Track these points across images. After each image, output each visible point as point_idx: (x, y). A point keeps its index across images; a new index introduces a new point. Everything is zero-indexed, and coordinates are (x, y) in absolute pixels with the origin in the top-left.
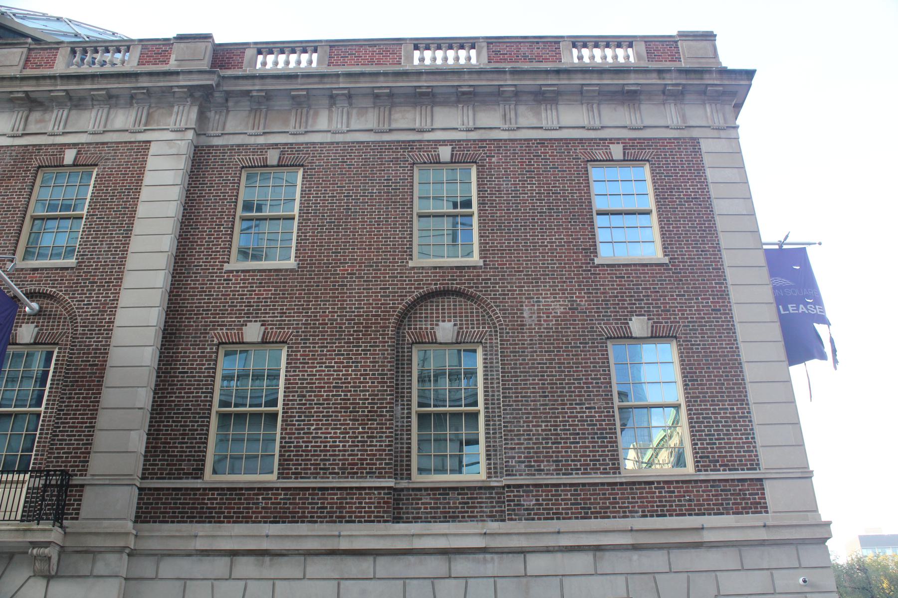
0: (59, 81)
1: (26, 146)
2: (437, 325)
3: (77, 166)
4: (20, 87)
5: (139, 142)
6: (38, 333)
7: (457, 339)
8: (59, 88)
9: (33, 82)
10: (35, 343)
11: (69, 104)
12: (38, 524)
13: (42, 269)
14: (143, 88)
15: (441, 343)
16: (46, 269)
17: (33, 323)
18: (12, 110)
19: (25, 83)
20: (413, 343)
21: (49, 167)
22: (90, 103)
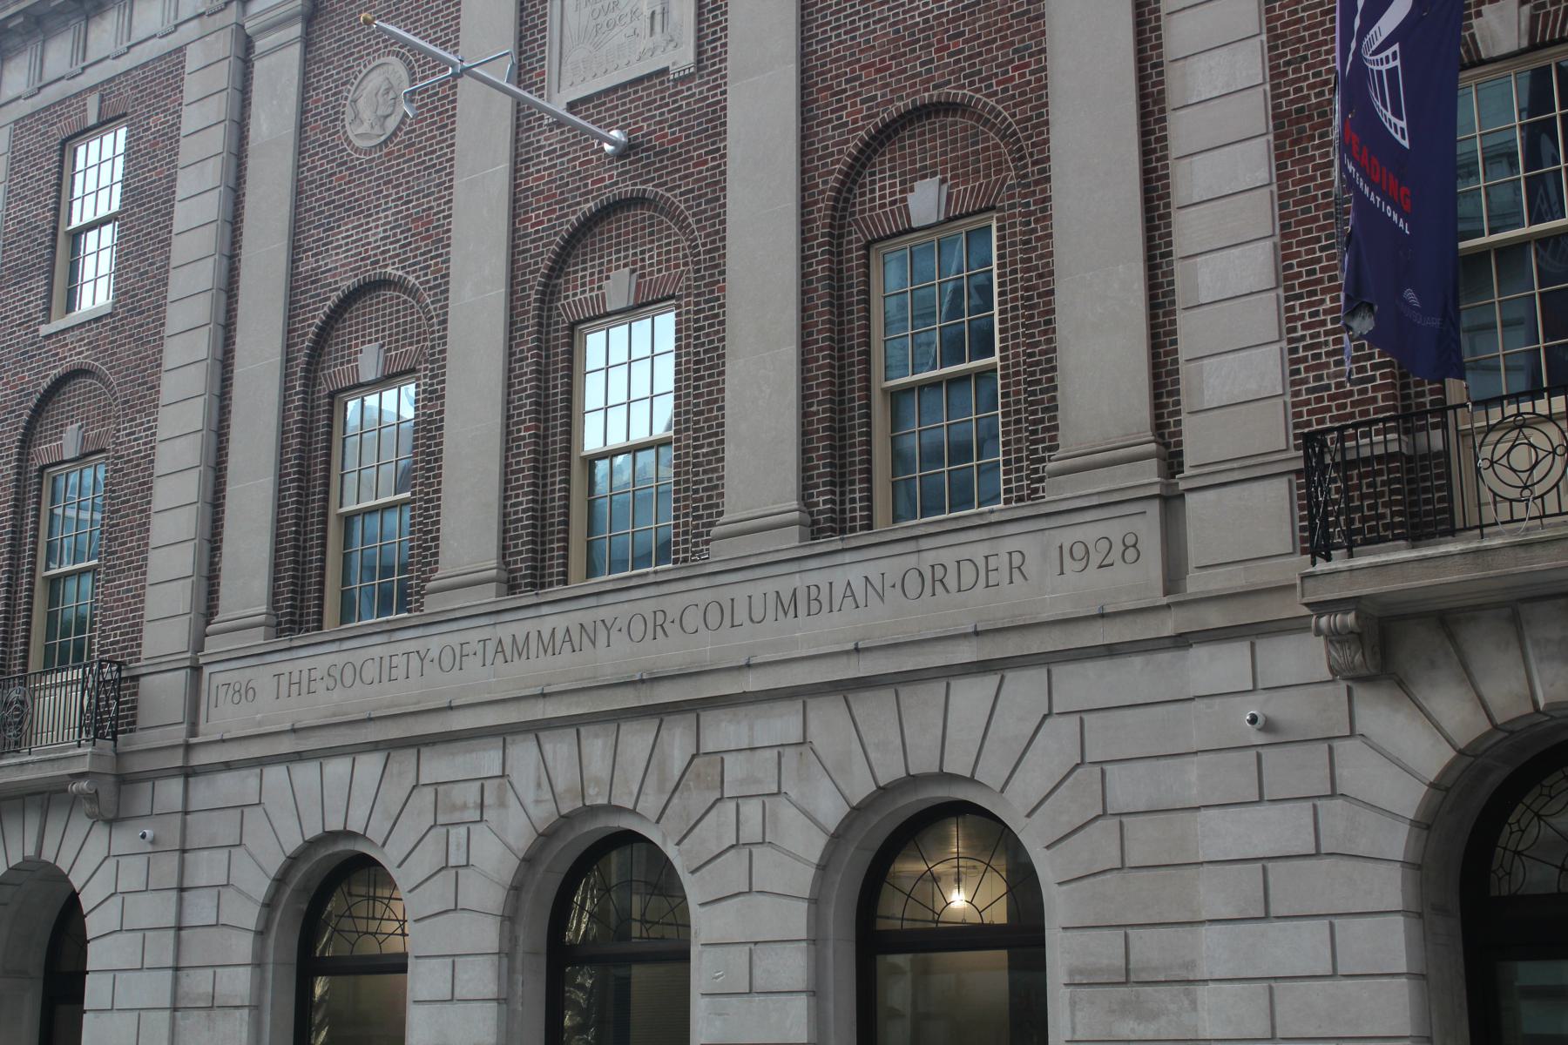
6: (1534, 19)
10: (1533, 47)
12: (1351, 556)
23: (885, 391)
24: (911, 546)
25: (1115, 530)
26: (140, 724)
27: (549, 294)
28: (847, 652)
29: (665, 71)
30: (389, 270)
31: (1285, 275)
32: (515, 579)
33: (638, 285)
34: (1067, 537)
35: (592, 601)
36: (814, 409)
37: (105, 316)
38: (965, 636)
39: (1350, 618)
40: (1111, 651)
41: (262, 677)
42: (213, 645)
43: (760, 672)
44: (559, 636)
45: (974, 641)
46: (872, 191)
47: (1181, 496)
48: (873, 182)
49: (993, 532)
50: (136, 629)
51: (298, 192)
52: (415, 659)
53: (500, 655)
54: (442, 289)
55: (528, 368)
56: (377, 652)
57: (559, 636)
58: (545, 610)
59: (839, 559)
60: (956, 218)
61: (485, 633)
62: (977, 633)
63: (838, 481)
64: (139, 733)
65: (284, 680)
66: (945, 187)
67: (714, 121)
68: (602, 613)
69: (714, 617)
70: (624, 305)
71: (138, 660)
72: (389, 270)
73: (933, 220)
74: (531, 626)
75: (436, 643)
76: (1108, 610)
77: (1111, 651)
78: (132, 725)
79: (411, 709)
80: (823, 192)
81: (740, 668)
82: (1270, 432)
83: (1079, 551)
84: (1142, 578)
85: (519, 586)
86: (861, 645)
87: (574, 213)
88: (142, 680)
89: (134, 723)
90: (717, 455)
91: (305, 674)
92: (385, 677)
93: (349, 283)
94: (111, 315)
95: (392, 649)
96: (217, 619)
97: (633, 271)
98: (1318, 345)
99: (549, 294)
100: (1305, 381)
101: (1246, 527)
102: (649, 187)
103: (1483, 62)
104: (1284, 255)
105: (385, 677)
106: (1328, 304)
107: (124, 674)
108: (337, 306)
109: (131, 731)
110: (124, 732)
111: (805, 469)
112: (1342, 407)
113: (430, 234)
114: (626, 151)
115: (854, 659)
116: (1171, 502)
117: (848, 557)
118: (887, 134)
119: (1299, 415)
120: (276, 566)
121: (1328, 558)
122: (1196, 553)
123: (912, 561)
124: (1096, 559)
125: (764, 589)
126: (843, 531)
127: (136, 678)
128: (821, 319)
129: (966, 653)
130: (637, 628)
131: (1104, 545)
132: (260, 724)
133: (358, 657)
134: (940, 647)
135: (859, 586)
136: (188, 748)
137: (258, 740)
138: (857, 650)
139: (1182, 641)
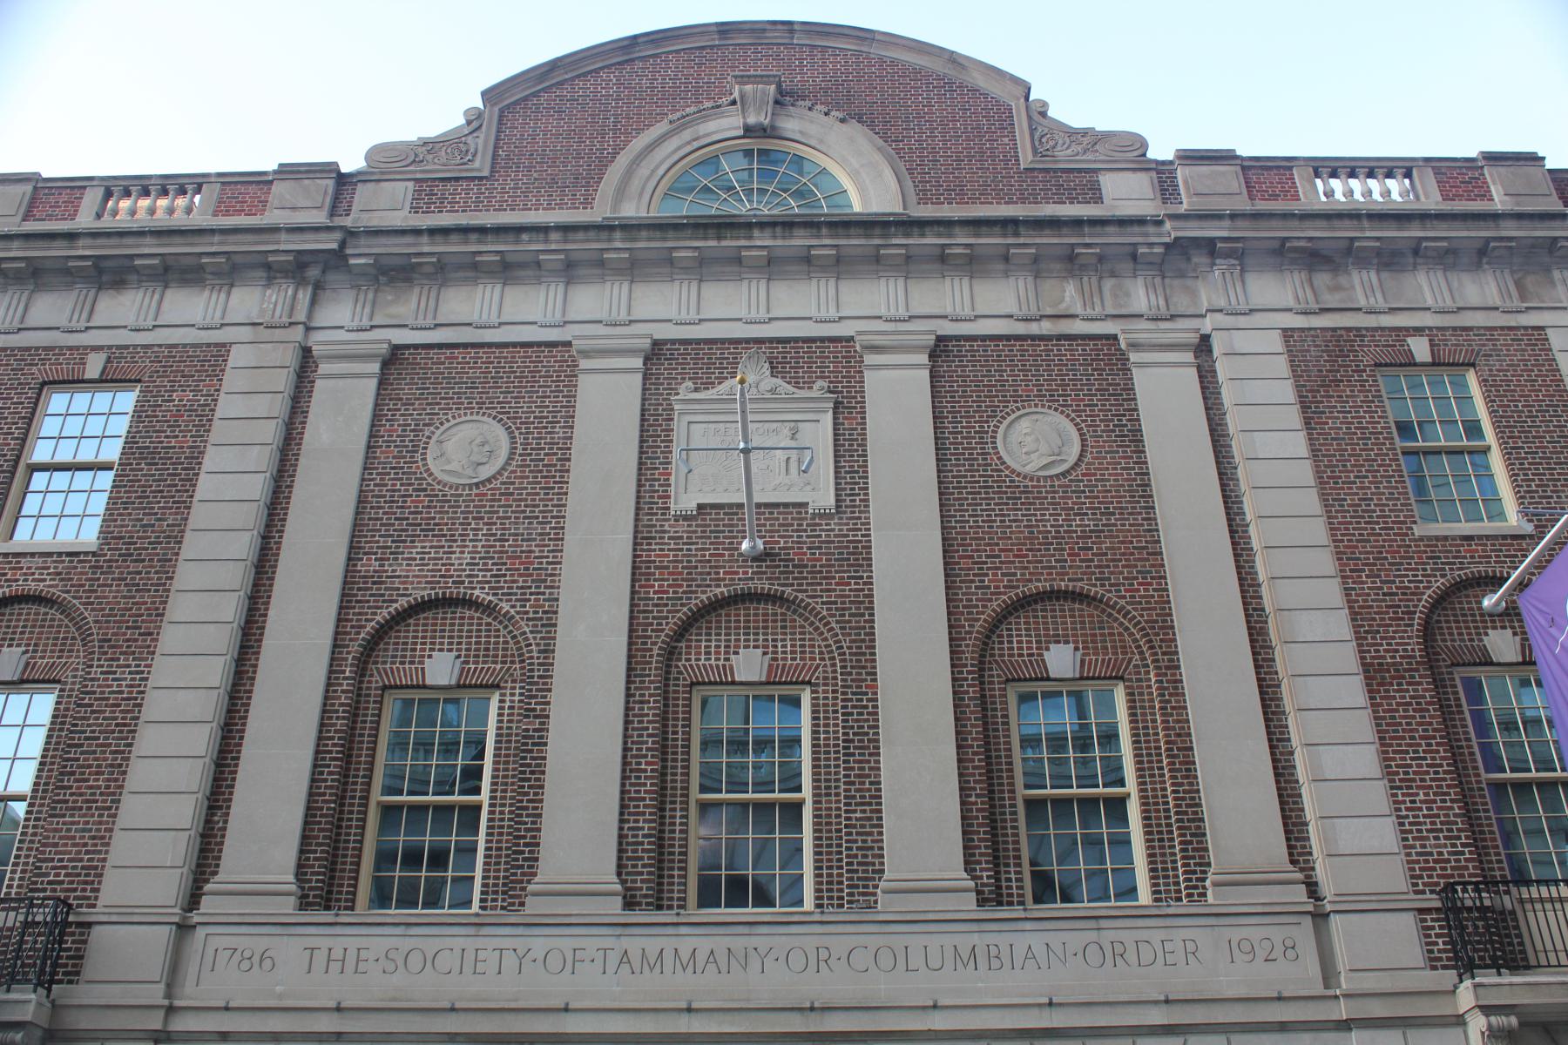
0: (1366, 223)
1: (1334, 330)
2: (1048, 649)
3: (1439, 365)
4: (1302, 230)
5: (1526, 328)
7: (1082, 671)
8: (1368, 234)
9: (1323, 223)
11: (1375, 261)
13: (1480, 537)
14: (1510, 239)
15: (1055, 680)
16: (1488, 537)
17: (1503, 628)
18: (1279, 269)
19: (1307, 224)
20: (1008, 680)
21: (1391, 365)
22: (1411, 260)
23: (378, 803)
24: (1092, 924)
25: (1277, 934)
26: (88, 972)
27: (671, 654)
28: (1040, 1005)
29: (805, 505)
30: (476, 592)
31: (1389, 774)
32: (634, 896)
33: (770, 666)
34: (1236, 934)
35: (745, 930)
36: (973, 799)
37: (86, 553)
38: (1156, 1002)
39: (1514, 1020)
40: (1283, 1027)
41: (290, 949)
42: (207, 904)
43: (945, 1013)
44: (701, 957)
45: (1164, 1007)
46: (1010, 642)
47: (1328, 915)
48: (1010, 636)
49: (1168, 922)
50: (93, 875)
51: (361, 501)
52: (510, 961)
53: (711, 967)
54: (547, 622)
55: (650, 711)
56: (458, 943)
57: (701, 957)
58: (683, 930)
59: (1020, 925)
60: (1088, 678)
61: (608, 943)
62: (1167, 1001)
63: (996, 862)
64: (82, 987)
65: (320, 958)
66: (1079, 654)
67: (858, 556)
68: (755, 941)
69: (886, 960)
70: (756, 679)
71: (94, 906)
72: (476, 592)
73: (1070, 675)
74: (668, 944)
75: (538, 944)
76: (1285, 994)
77: (1283, 1027)
78: (73, 976)
79: (513, 1005)
80: (970, 633)
81: (924, 1008)
82: (1393, 877)
83: (1246, 946)
84: (1304, 973)
85: (639, 904)
86: (694, 1005)
87: (704, 592)
88: (96, 930)
89: (78, 973)
90: (875, 819)
91: (352, 954)
92: (468, 969)
93: (422, 593)
94: (94, 554)
95: (480, 942)
96: (217, 878)
97: (765, 653)
98: (1420, 824)
99: (671, 654)
100: (1413, 847)
101: (1385, 946)
102: (788, 590)
103: (1492, 664)
104: (1385, 759)
105: (468, 969)
106: (1422, 797)
107: (71, 918)
108: (405, 610)
109: (70, 982)
110: (60, 982)
111: (967, 847)
112: (1444, 869)
113: (538, 577)
114: (758, 558)
115: (1046, 1012)
116: (1320, 917)
117: (1028, 925)
118: (1024, 603)
119: (1413, 869)
120: (305, 838)
121: (1499, 974)
122: (1342, 962)
123: (1093, 935)
124: (1261, 954)
125: (939, 942)
126: (1000, 903)
127: (90, 925)
128: (974, 731)
129: (1157, 1017)
130: (797, 960)
131: (1267, 944)
132: (280, 996)
133: (431, 946)
134: (1131, 1009)
135: (1039, 950)
136: (171, 1010)
137: (277, 1014)
138: (1167, 1001)
139: (1345, 1025)
